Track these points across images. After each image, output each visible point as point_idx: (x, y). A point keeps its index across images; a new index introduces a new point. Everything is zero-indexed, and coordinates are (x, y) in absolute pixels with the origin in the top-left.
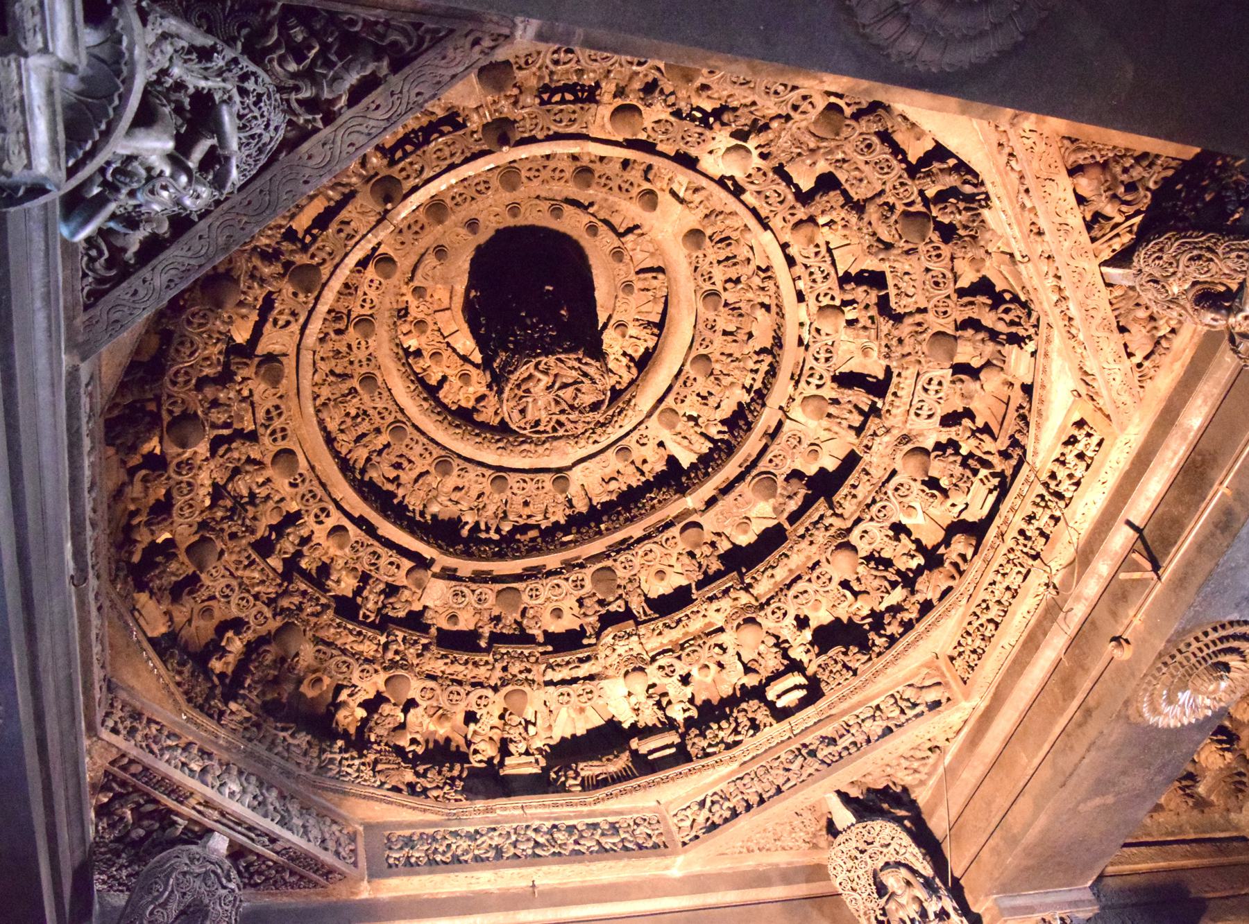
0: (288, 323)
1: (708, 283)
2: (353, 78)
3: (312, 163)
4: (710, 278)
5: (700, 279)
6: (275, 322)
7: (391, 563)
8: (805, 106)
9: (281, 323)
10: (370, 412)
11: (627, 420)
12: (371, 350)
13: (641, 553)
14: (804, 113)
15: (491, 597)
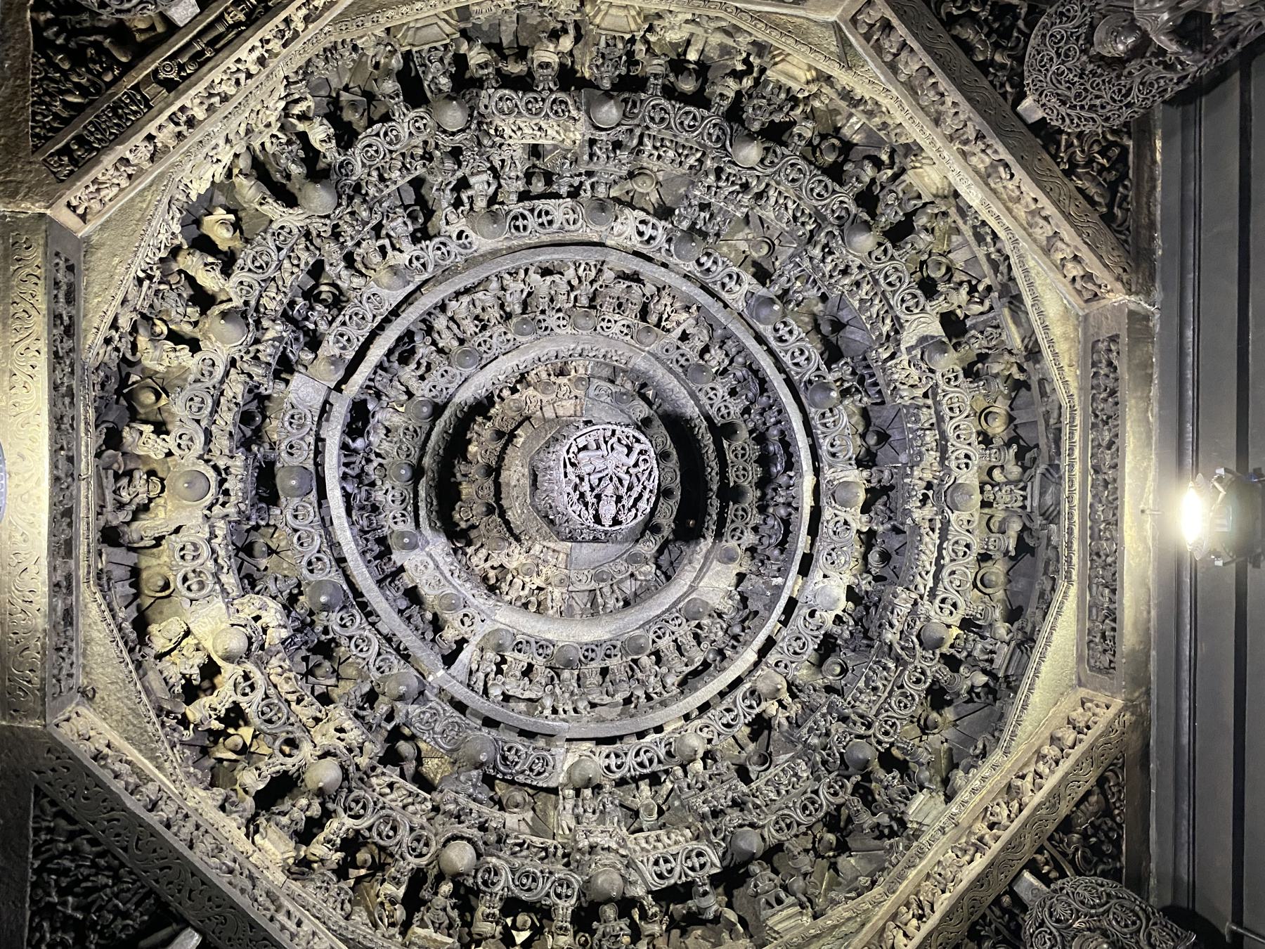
0: (641, 234)
1: (654, 636)
2: (1092, 190)
3: (1036, 162)
4: (659, 637)
5: (654, 628)
6: (642, 222)
7: (349, 340)
8: (948, 607)
9: (642, 228)
10: (487, 334)
11: (482, 601)
12: (557, 330)
13: (366, 633)
14: (941, 609)
15: (295, 461)
